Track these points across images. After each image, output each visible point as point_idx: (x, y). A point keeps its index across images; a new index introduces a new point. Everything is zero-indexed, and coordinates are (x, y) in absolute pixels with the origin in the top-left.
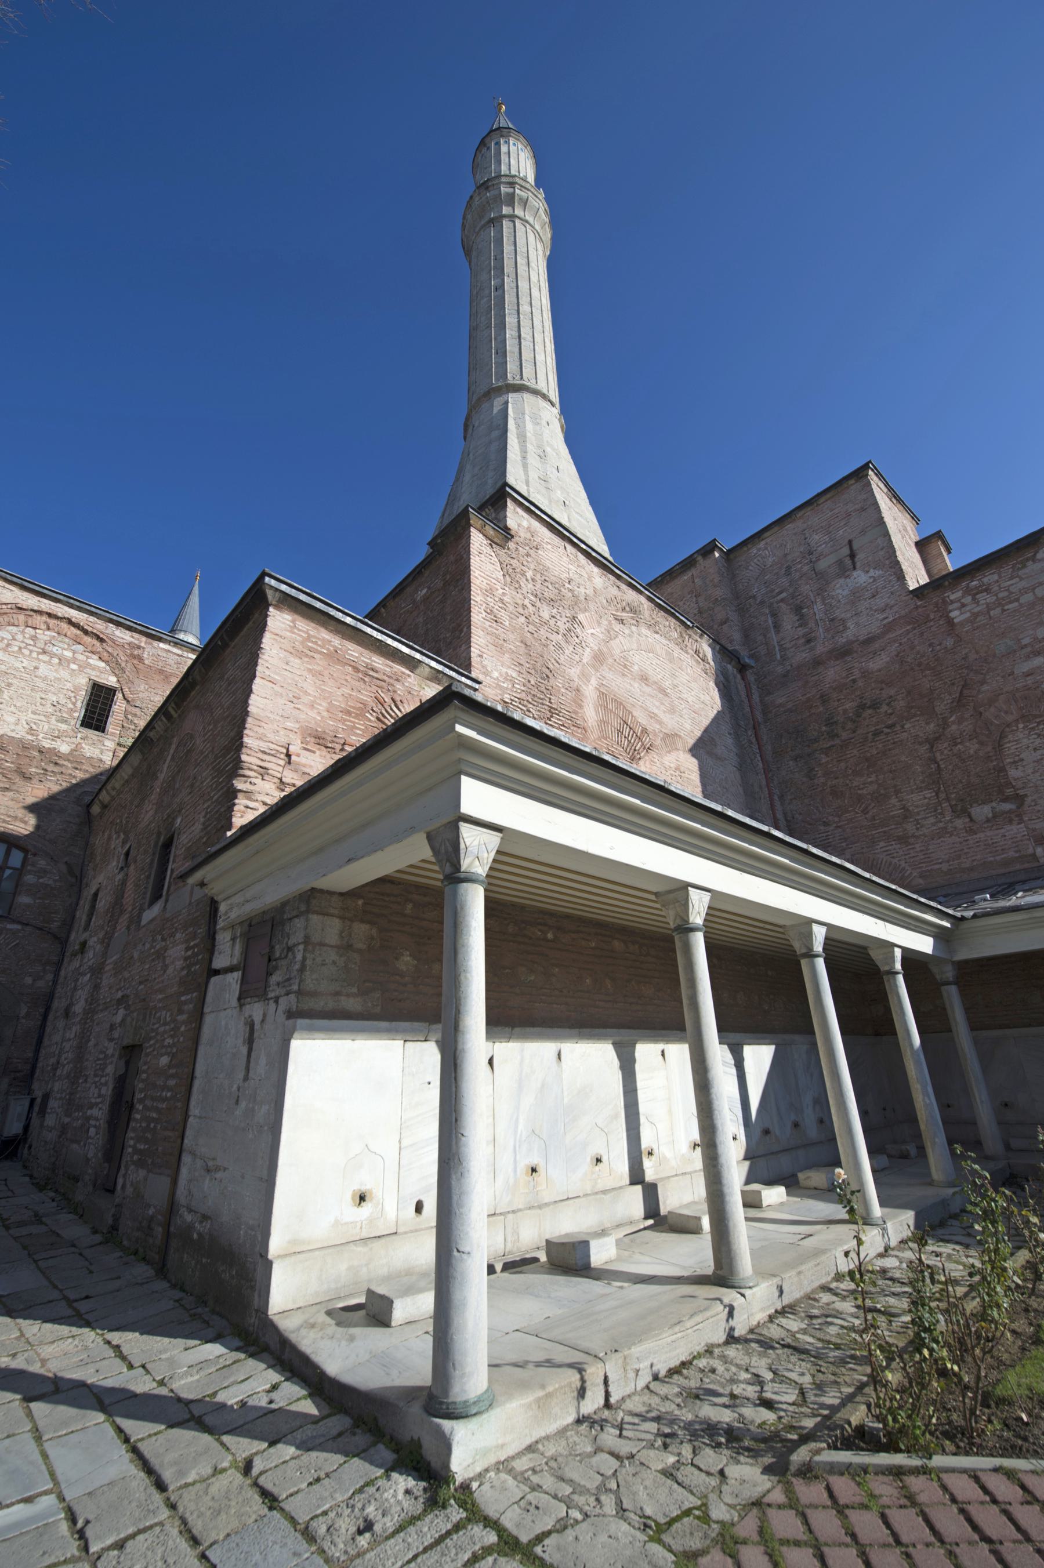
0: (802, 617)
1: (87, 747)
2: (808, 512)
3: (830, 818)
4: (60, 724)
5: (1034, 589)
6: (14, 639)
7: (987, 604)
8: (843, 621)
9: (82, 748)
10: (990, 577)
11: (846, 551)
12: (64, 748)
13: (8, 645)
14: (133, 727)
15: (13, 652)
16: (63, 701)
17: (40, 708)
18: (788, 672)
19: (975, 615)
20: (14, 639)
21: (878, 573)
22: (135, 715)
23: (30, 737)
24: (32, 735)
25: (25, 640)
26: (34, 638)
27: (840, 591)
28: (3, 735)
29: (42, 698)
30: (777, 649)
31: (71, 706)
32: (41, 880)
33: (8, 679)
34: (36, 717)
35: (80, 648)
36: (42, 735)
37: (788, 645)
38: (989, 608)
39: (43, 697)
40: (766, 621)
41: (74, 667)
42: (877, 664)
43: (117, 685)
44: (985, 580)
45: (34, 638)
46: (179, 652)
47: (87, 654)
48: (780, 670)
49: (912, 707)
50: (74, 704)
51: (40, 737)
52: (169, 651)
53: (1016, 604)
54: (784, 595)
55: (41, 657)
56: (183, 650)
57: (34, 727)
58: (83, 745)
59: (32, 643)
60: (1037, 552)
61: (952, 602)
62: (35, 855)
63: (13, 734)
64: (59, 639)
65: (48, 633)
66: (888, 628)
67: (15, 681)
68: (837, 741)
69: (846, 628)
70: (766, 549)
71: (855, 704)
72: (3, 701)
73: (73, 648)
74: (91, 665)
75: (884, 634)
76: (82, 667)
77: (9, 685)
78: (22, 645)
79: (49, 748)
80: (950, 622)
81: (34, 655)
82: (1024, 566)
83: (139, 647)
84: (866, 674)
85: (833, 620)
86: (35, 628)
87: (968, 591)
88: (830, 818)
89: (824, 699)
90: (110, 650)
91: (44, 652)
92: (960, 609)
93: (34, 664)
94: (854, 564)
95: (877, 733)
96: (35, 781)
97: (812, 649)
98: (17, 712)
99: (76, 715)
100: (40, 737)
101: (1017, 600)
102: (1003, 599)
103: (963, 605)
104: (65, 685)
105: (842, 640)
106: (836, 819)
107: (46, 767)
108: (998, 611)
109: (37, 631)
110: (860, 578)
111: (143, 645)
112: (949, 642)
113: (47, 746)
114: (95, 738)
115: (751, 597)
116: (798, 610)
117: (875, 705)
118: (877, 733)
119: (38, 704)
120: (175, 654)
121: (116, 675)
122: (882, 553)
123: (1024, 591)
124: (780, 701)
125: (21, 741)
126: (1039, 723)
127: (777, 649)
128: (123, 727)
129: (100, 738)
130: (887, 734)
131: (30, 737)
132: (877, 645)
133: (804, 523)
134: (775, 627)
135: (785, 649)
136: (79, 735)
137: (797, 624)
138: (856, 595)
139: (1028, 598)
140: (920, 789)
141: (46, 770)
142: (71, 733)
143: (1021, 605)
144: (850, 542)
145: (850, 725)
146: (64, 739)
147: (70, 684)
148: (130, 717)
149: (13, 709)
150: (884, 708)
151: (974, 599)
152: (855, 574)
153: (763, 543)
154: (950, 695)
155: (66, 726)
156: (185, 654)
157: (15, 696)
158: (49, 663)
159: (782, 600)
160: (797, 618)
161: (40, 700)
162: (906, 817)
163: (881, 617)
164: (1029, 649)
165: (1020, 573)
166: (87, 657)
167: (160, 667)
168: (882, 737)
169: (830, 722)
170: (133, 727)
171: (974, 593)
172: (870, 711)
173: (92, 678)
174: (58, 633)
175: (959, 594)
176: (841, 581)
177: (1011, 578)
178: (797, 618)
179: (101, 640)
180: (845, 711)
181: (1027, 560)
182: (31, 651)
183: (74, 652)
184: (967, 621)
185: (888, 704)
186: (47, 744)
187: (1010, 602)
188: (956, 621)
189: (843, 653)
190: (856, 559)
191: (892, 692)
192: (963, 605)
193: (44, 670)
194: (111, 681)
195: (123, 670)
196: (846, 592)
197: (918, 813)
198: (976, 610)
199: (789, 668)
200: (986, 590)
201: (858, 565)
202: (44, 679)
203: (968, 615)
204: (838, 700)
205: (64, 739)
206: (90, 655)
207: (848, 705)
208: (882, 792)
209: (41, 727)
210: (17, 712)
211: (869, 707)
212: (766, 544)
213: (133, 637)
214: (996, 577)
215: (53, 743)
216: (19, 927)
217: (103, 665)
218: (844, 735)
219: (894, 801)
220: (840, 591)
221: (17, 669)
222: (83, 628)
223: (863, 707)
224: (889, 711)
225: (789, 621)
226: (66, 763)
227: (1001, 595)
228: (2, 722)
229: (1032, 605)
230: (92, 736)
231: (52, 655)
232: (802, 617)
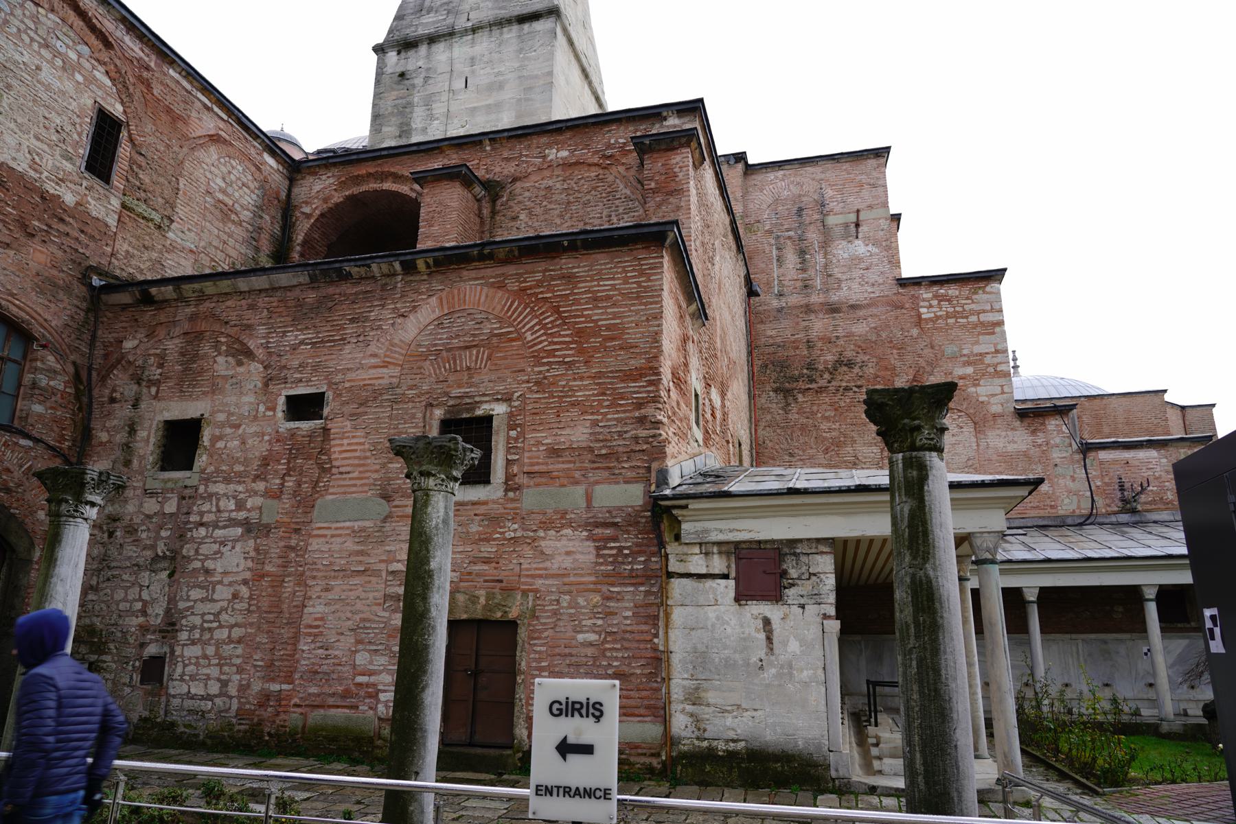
0: (804, 261)
1: (93, 202)
2: (829, 165)
3: (796, 451)
4: (64, 162)
5: (979, 314)
6: (12, 14)
7: (947, 312)
8: (839, 281)
9: (88, 202)
10: (952, 291)
11: (853, 217)
12: (69, 199)
13: (6, 22)
14: (138, 183)
15: (11, 34)
16: (68, 128)
17: (42, 131)
18: (782, 308)
19: (938, 318)
20: (12, 14)
21: (875, 250)
22: (140, 167)
23: (32, 173)
24: (35, 170)
25: (26, 20)
26: (35, 19)
27: (841, 252)
28: (3, 163)
29: (45, 117)
30: (776, 283)
31: (75, 136)
32: (52, 383)
33: (6, 77)
34: (38, 144)
35: (85, 50)
36: (46, 174)
37: (786, 283)
38: (948, 316)
39: (47, 115)
40: (771, 251)
41: (79, 78)
42: (860, 329)
43: (123, 118)
44: (950, 292)
45: (35, 19)
46: (188, 87)
47: (93, 62)
48: (775, 303)
49: (878, 377)
50: (80, 134)
51: (43, 176)
52: (178, 82)
53: (965, 320)
54: (791, 233)
55: (43, 51)
56: (193, 86)
57: (37, 159)
58: (89, 198)
59: (33, 27)
60: (987, 285)
61: (924, 300)
62: (44, 346)
63: (13, 165)
64: (64, 30)
65: (51, 16)
66: (872, 303)
67: (14, 82)
68: (813, 386)
69: (839, 288)
70: (783, 180)
71: (836, 358)
72: (2, 110)
73: (79, 48)
74: (97, 80)
75: (869, 306)
76: (90, 80)
77: (9, 87)
78: (22, 27)
79: (53, 195)
80: (919, 315)
81: (35, 46)
82: (976, 293)
83: (148, 68)
84: (849, 335)
85: (830, 275)
86: (37, 5)
87: (935, 296)
88: (796, 451)
89: (810, 344)
90: (118, 62)
91: (47, 46)
92: (928, 308)
93: (37, 62)
94: (857, 232)
95: (847, 389)
96: (36, 239)
97: (808, 295)
98: (18, 131)
99: (81, 151)
100: (43, 176)
101: (967, 317)
102: (958, 312)
103: (931, 306)
104: (70, 104)
105: (834, 298)
106: (801, 453)
107: (50, 222)
108: (951, 321)
109: (40, 10)
110: (860, 248)
111: (152, 64)
112: (915, 332)
113: (52, 191)
114: (102, 191)
115: (759, 222)
116: (802, 253)
117: (850, 364)
118: (847, 389)
119: (41, 125)
120: (184, 88)
121: (122, 103)
122: (881, 233)
123: (972, 312)
124: (769, 333)
125: (22, 177)
126: (959, 416)
127: (776, 283)
128: (128, 180)
129: (107, 193)
130: (855, 392)
131: (32, 173)
132: (861, 313)
133: (822, 172)
134: (778, 260)
135: (783, 285)
136: (85, 183)
137: (799, 266)
138: (856, 260)
139: (973, 319)
140: (870, 444)
141: (50, 227)
142: (76, 179)
143: (968, 323)
144: (858, 211)
145: (826, 376)
146: (69, 185)
147: (74, 104)
148: (134, 167)
149: (12, 125)
150: (856, 370)
151: (939, 304)
152: (857, 242)
153: (782, 172)
154: (907, 375)
155: (71, 166)
156: (195, 92)
157: (15, 108)
158: (51, 63)
159: (790, 238)
160: (799, 260)
161: (41, 118)
162: (855, 464)
163: (870, 290)
164: (966, 359)
165: (974, 297)
166: (94, 68)
167: (167, 103)
168: (850, 394)
169: (810, 366)
170: (138, 183)
171: (941, 299)
172: (845, 368)
173: (98, 99)
174: (63, 20)
175: (930, 295)
176: (844, 243)
177: (967, 298)
178: (799, 260)
179: (108, 45)
180: (826, 362)
181: (980, 288)
182: (32, 40)
183: (80, 55)
184: (930, 319)
185: (861, 367)
186: (51, 188)
187: (962, 318)
188: (923, 316)
189: (833, 309)
190: (860, 229)
191: (866, 358)
192: (931, 306)
193: (46, 74)
194: (117, 109)
195: (130, 95)
196: (846, 256)
197: (865, 463)
198: (938, 314)
199: (784, 305)
200: (948, 300)
201: (860, 235)
202: (48, 87)
203: (932, 315)
204: (822, 350)
205: (69, 185)
206: (96, 64)
207: (829, 357)
208: (842, 439)
209: (44, 161)
210: (18, 131)
211: (845, 365)
212: (785, 175)
213: (143, 51)
214: (957, 293)
215: (57, 188)
216: (30, 443)
217: (108, 83)
218: (822, 383)
219: (849, 449)
220: (841, 252)
221: (16, 63)
222: (90, 19)
223: (839, 363)
224: (860, 374)
225: (791, 258)
226: (71, 220)
227: (957, 309)
228: (1, 144)
229: (975, 326)
230: (99, 188)
231: (57, 54)
232: (804, 261)
